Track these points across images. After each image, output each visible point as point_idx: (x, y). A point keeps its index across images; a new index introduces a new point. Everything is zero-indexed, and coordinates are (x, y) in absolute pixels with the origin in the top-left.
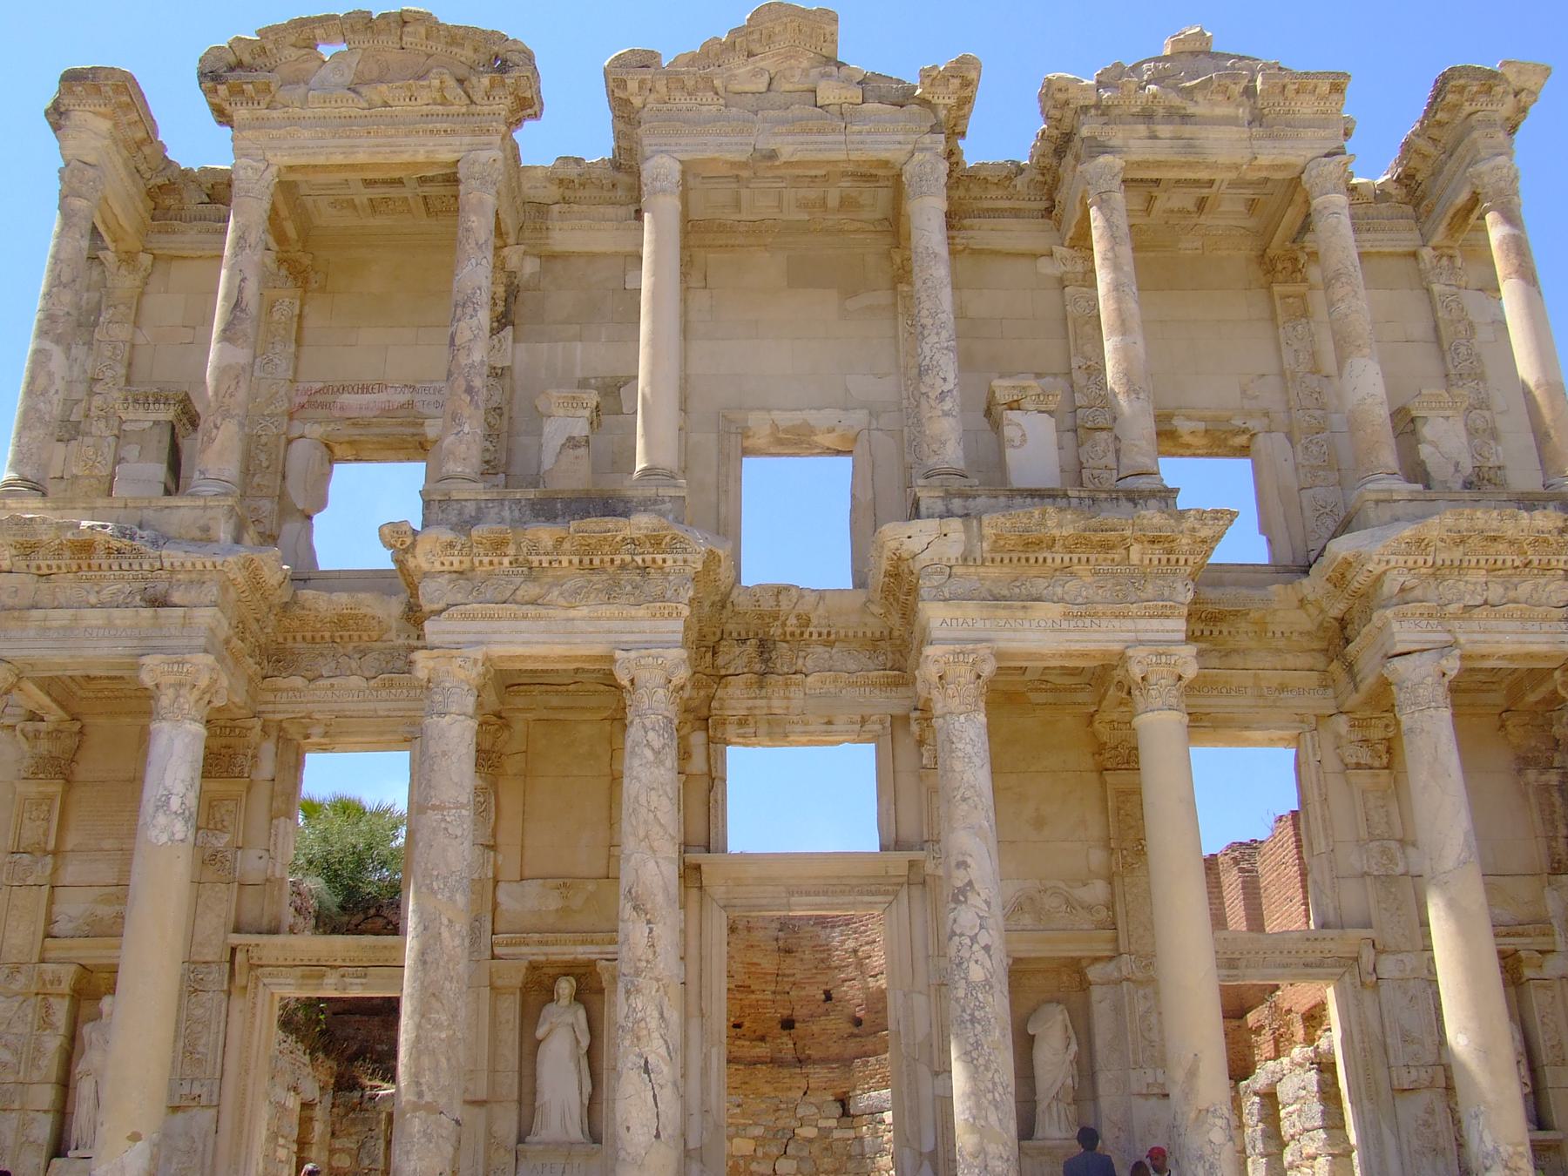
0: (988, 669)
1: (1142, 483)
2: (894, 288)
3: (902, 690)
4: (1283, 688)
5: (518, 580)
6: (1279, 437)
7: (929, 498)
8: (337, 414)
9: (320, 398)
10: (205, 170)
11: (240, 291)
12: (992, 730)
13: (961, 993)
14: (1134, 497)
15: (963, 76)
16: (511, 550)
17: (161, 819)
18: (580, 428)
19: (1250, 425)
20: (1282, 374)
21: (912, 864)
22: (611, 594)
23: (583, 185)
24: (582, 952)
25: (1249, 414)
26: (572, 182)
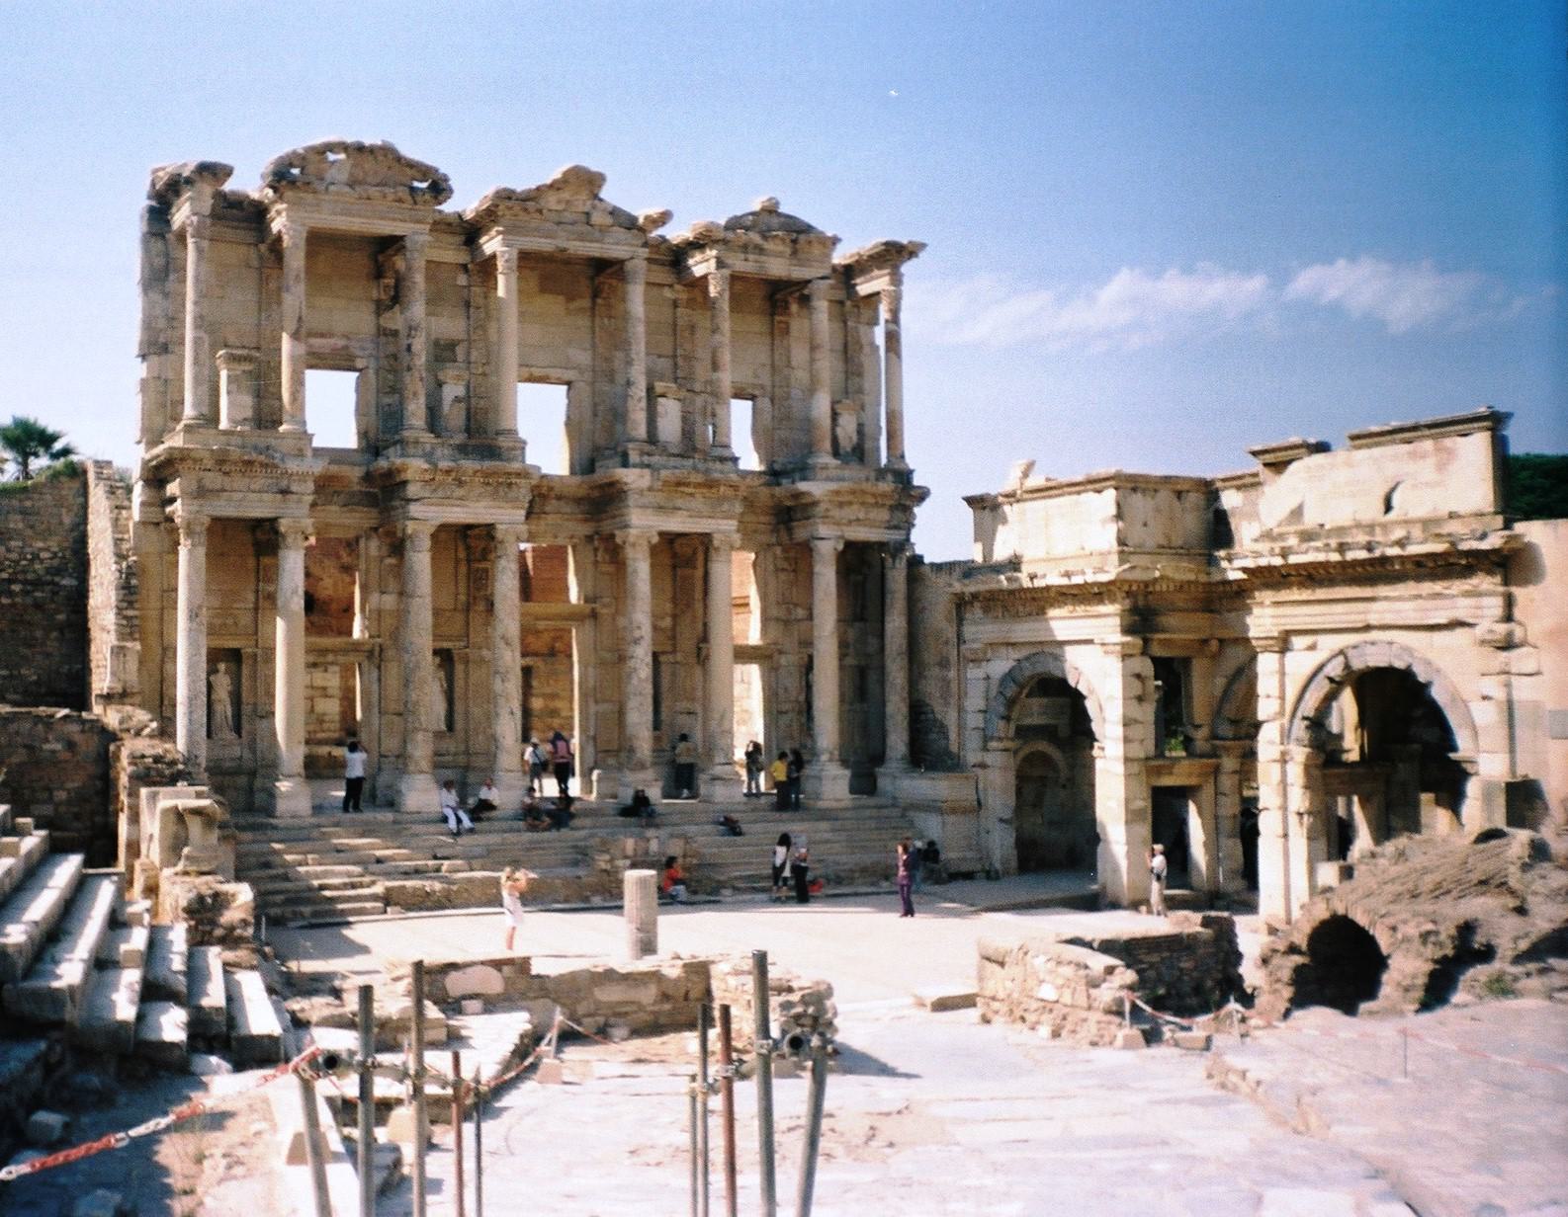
0: (655, 540)
1: (725, 453)
2: (595, 295)
4: (755, 531)
6: (767, 401)
7: (634, 457)
12: (652, 566)
14: (722, 460)
15: (664, 218)
17: (296, 599)
18: (460, 391)
19: (757, 392)
20: (773, 366)
21: (593, 610)
22: (495, 496)
24: (446, 645)
25: (754, 386)
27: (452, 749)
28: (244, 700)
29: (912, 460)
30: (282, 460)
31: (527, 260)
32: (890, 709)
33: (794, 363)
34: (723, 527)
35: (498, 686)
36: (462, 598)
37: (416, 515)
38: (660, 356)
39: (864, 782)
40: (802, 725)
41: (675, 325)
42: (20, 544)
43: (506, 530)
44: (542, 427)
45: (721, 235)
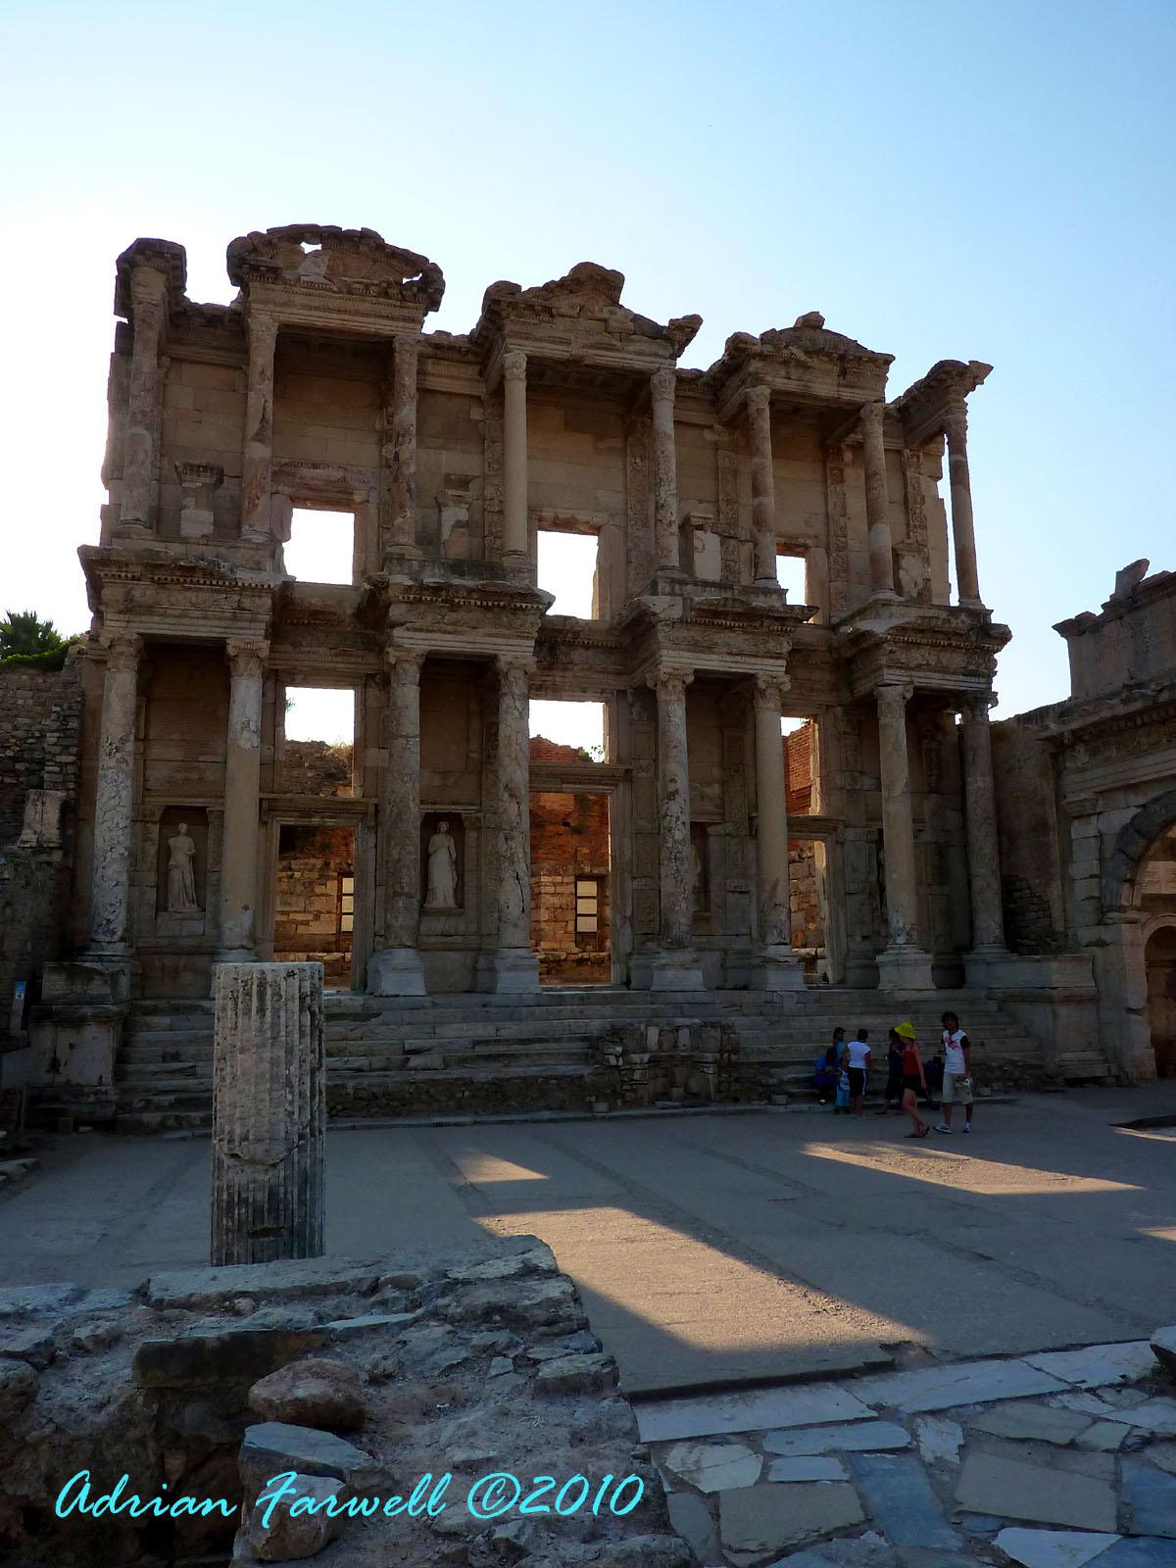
0: (690, 679)
1: (769, 584)
3: (624, 677)
5: (444, 611)
6: (822, 551)
8: (297, 480)
9: (287, 469)
10: (207, 305)
11: (264, 409)
13: (670, 845)
16: (444, 593)
17: (246, 734)
18: (462, 514)
19: (809, 542)
20: (827, 515)
23: (448, 349)
24: (453, 809)
25: (807, 536)
26: (443, 346)
27: (462, 928)
28: (209, 867)
29: (988, 597)
30: (232, 571)
31: (537, 369)
32: (978, 884)
33: (849, 512)
34: (770, 669)
35: (503, 847)
36: (474, 756)
37: (400, 641)
38: (701, 501)
39: (952, 972)
40: (874, 911)
41: (717, 467)
42: (27, 721)
43: (511, 663)
44: (568, 572)
45: (758, 348)
